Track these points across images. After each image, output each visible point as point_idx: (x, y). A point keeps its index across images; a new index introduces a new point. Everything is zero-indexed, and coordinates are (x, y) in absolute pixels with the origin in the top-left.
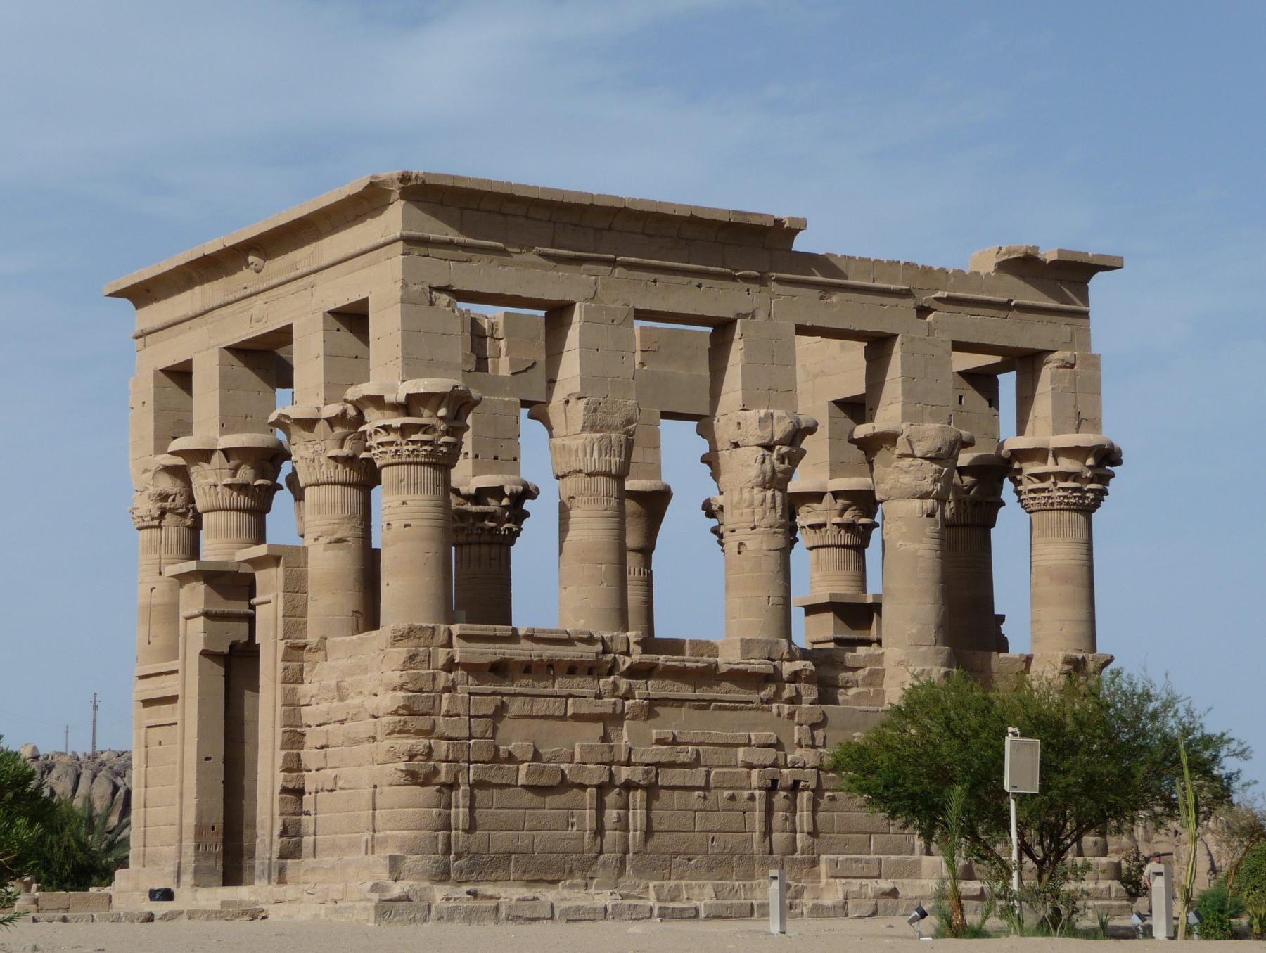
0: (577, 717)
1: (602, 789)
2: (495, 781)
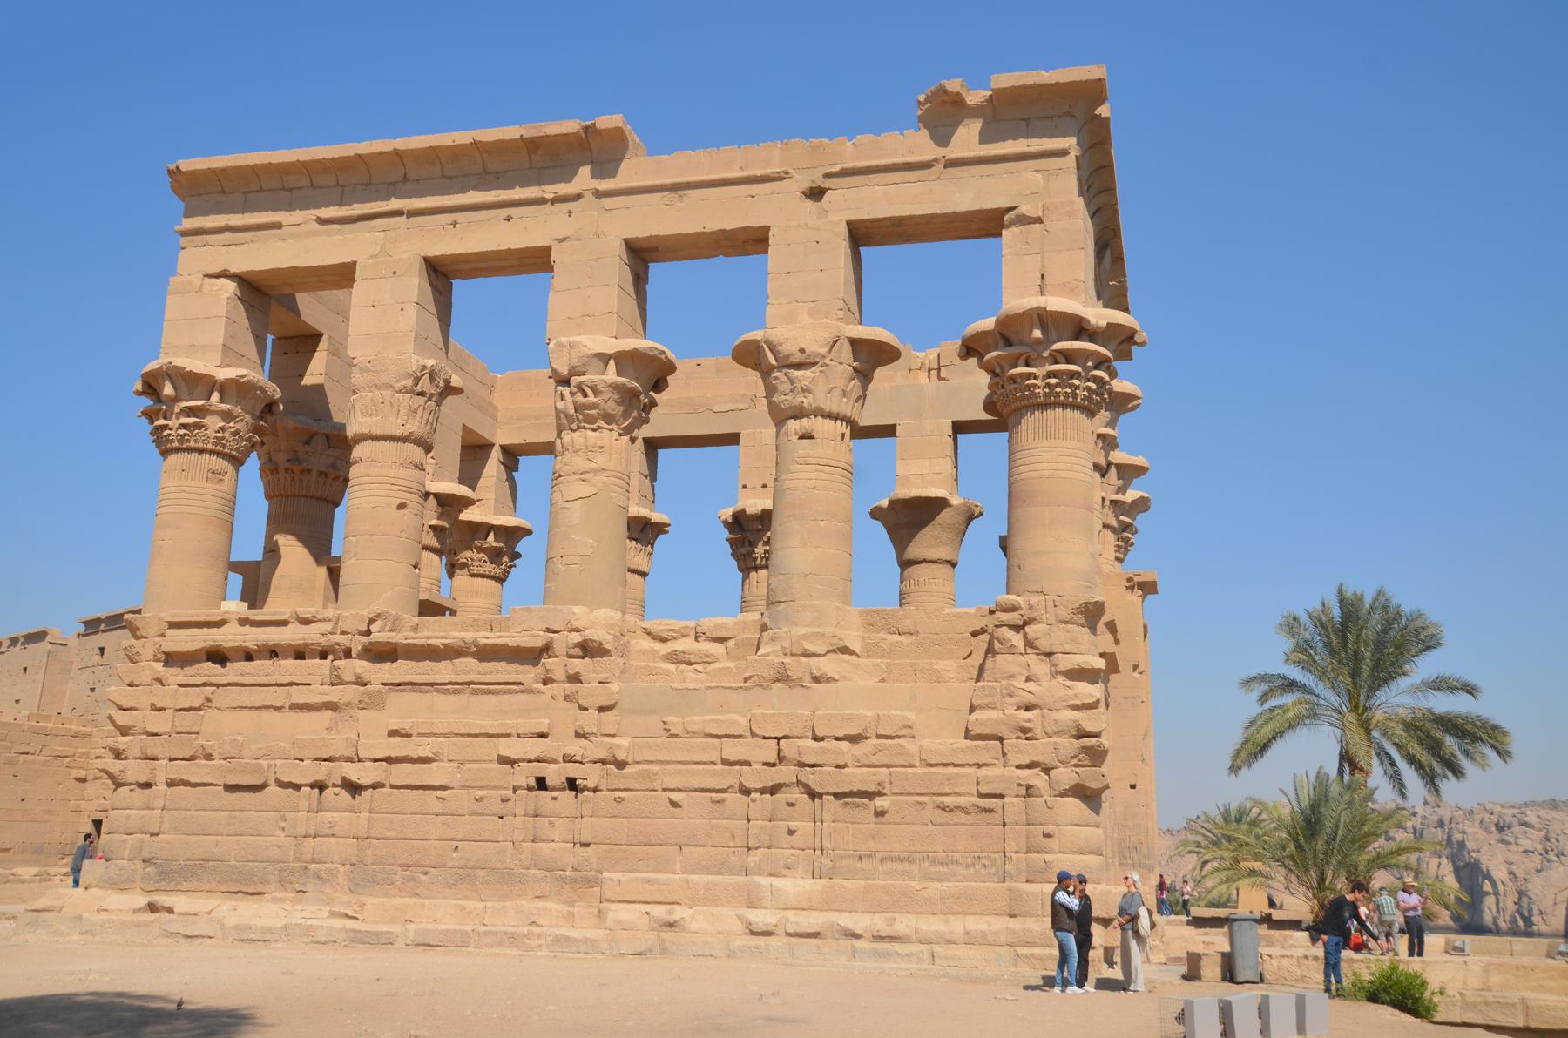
0: (295, 707)
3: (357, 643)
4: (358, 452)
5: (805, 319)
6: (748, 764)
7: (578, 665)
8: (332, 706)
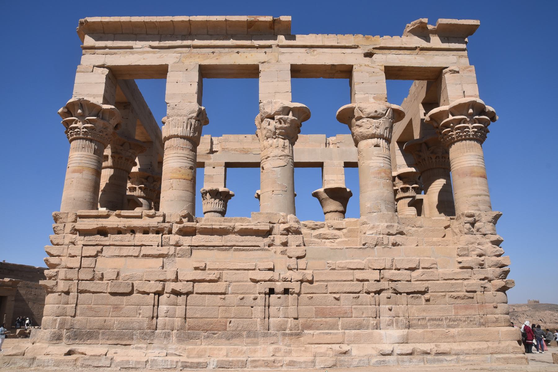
0: (145, 256)
1: (159, 294)
2: (92, 290)
3: (175, 229)
4: (167, 144)
5: (372, 100)
6: (368, 280)
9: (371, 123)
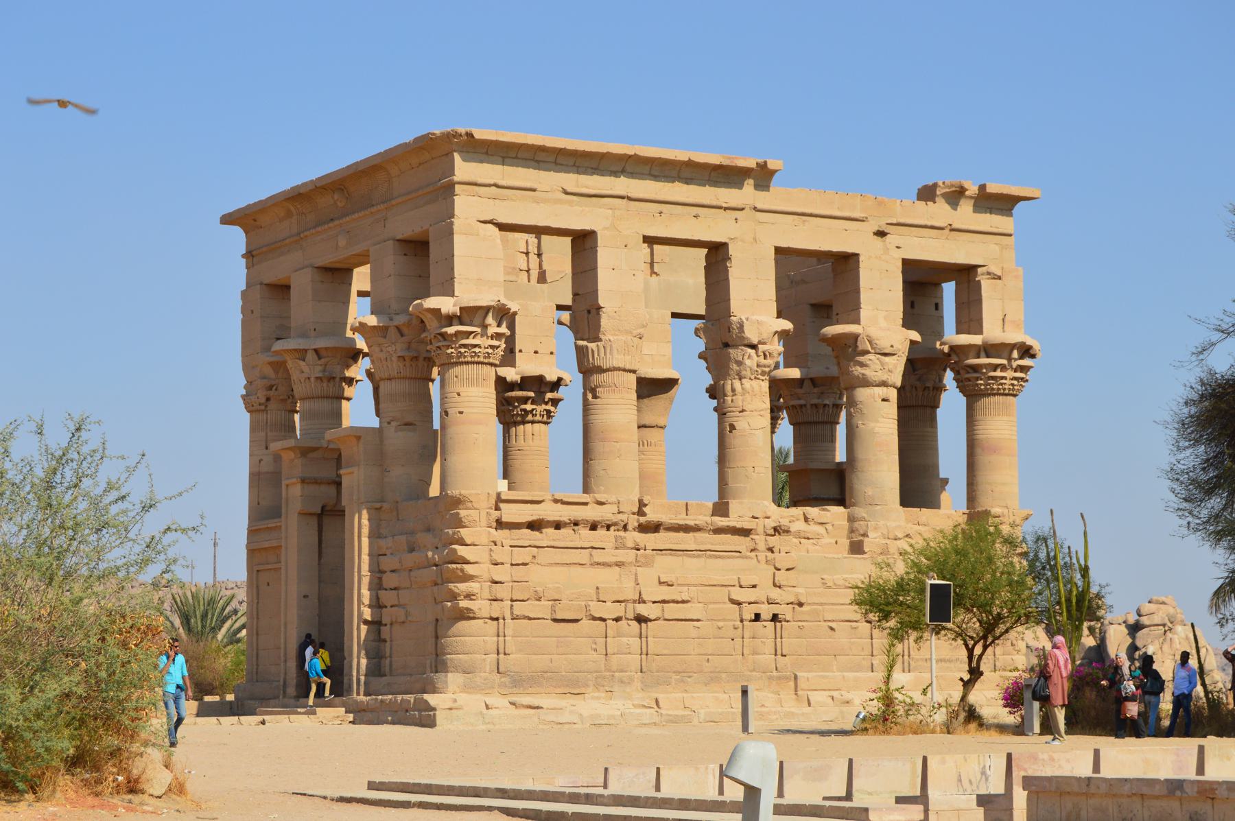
3: (633, 521)
7: (774, 541)
8: (619, 564)
9: (882, 364)
